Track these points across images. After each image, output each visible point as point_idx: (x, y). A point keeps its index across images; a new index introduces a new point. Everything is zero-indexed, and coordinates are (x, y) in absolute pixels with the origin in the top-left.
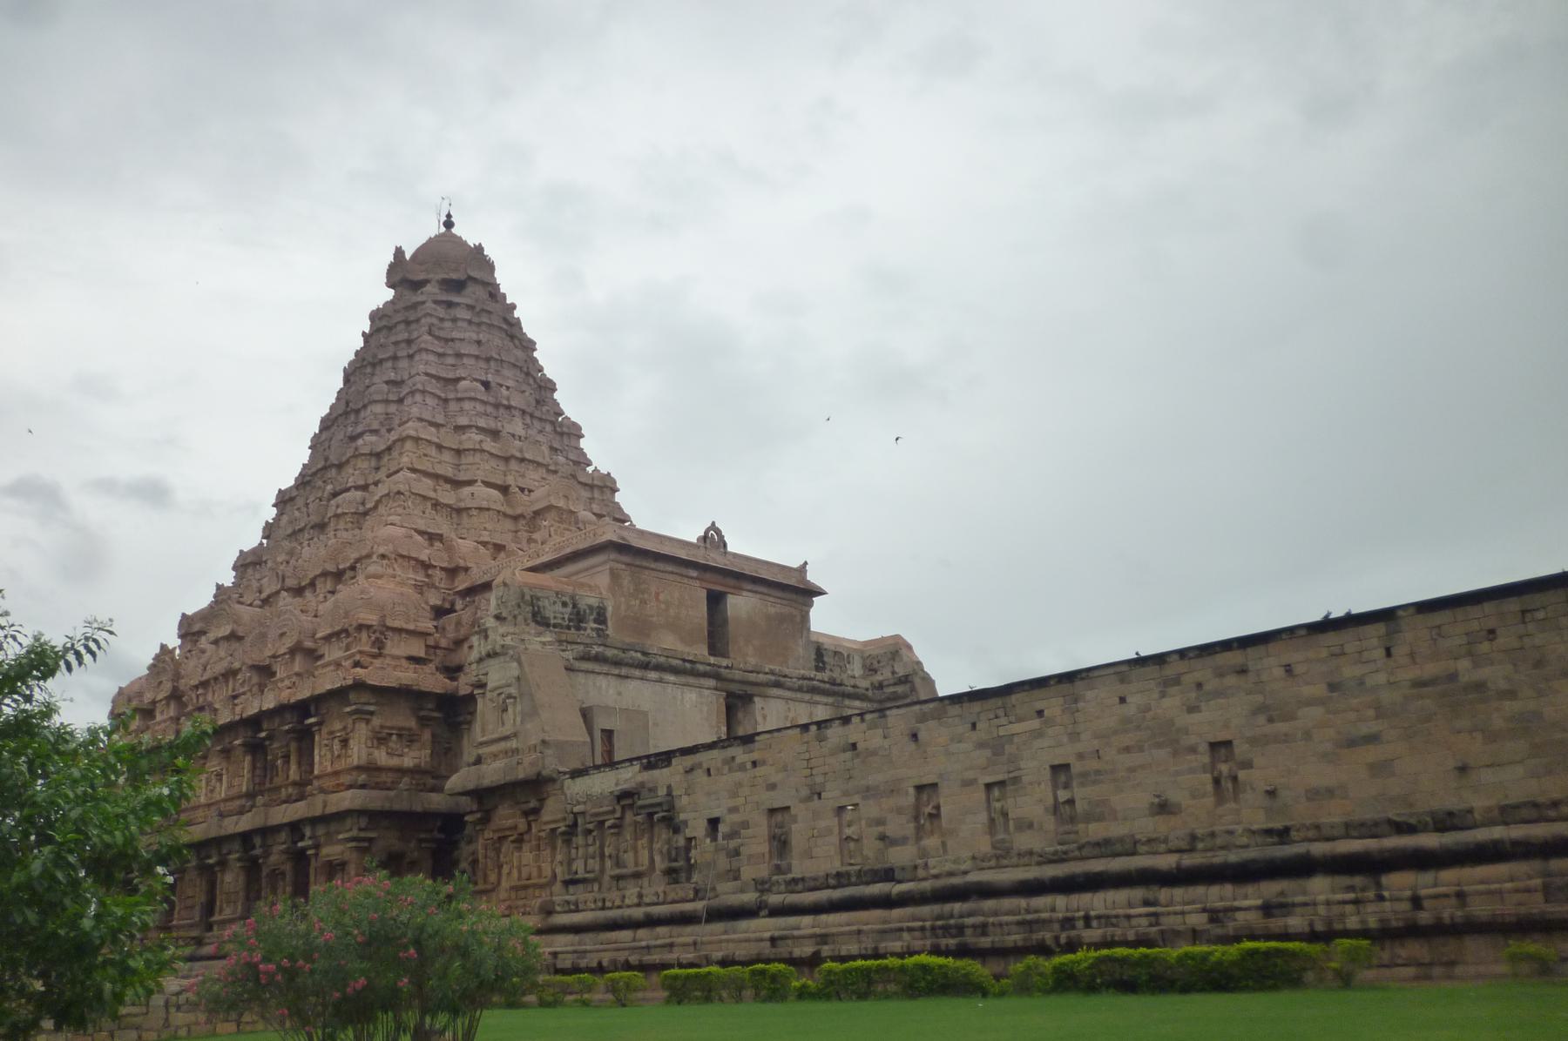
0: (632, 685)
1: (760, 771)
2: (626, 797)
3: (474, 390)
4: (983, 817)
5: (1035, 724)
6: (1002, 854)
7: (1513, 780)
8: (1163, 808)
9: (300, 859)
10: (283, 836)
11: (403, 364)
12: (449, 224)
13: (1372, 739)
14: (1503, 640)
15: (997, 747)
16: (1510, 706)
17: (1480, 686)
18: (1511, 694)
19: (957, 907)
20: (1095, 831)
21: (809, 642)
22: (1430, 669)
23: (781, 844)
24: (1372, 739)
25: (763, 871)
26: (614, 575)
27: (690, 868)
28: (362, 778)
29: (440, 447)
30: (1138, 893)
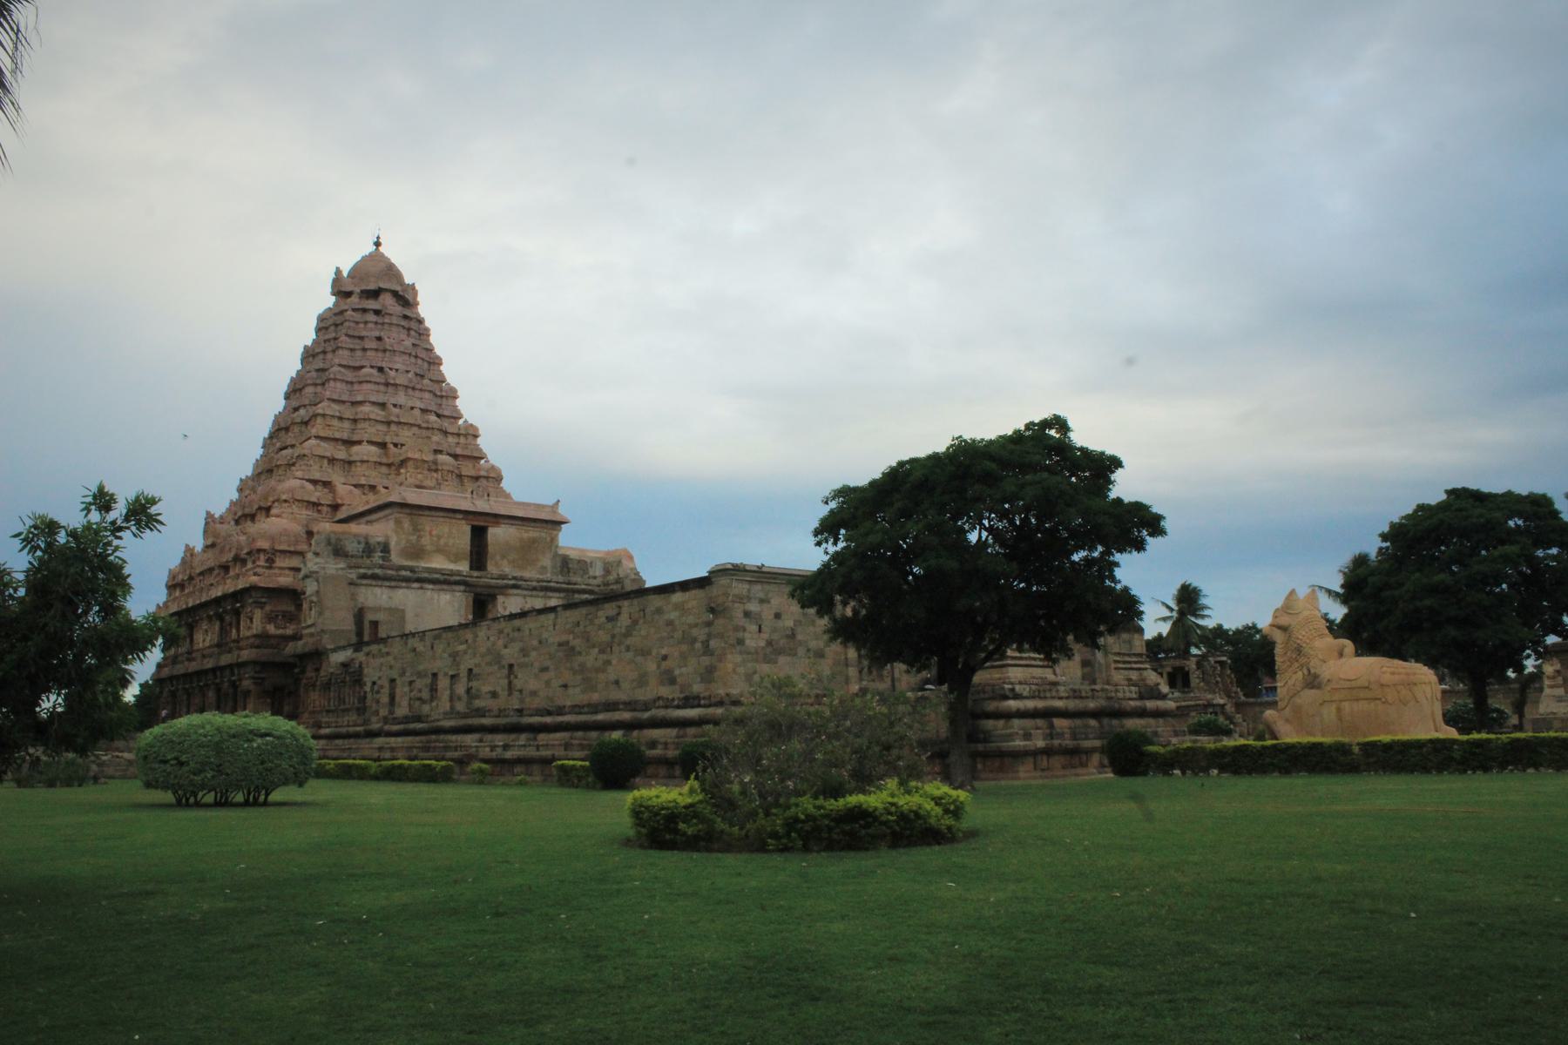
1: (390, 658)
2: (345, 665)
3: (371, 375)
5: (463, 647)
6: (452, 713)
7: (576, 696)
8: (494, 695)
9: (234, 685)
10: (227, 672)
11: (329, 356)
12: (378, 244)
15: (454, 655)
16: (580, 659)
17: (573, 648)
20: (478, 703)
21: (556, 554)
22: (564, 638)
23: (392, 697)
25: (383, 712)
26: (398, 522)
28: (257, 642)
29: (341, 418)
30: (476, 736)
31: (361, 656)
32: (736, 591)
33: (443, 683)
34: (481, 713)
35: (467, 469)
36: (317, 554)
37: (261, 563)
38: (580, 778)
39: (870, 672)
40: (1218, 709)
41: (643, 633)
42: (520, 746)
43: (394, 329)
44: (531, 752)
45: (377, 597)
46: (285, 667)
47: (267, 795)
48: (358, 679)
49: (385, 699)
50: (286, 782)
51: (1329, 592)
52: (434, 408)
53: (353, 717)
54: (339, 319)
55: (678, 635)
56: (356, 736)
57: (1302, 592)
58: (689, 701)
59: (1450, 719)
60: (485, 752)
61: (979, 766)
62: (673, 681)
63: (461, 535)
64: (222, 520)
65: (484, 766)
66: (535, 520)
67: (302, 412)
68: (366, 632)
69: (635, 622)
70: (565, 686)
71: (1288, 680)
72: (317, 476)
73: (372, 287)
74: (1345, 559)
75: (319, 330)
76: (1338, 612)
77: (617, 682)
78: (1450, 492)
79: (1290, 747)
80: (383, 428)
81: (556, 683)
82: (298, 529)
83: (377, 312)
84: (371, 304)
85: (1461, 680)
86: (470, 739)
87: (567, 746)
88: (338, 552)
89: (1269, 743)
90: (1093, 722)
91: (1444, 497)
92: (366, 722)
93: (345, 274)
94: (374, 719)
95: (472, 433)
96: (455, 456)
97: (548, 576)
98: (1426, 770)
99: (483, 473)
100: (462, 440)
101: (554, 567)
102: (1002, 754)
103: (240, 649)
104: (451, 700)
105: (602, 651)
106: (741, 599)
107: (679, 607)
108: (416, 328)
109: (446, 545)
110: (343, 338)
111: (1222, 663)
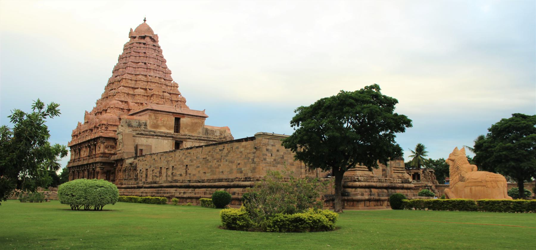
0: (150, 139)
2: (131, 164)
4: (165, 174)
6: (167, 181)
7: (208, 176)
9: (93, 170)
11: (128, 58)
12: (145, 20)
13: (199, 167)
14: (211, 153)
15: (168, 161)
16: (210, 164)
17: (208, 160)
18: (210, 162)
19: (160, 189)
20: (175, 178)
21: (204, 128)
22: (205, 156)
23: (147, 175)
24: (199, 167)
25: (144, 180)
26: (150, 116)
27: (137, 179)
28: (102, 155)
29: (131, 80)
30: (174, 189)
31: (136, 161)
32: (264, 142)
33: (164, 171)
34: (176, 181)
35: (174, 98)
36: (122, 126)
37: (104, 128)
38: (209, 204)
39: (309, 171)
40: (429, 188)
41: (232, 155)
42: (189, 193)
43: (150, 49)
44: (193, 195)
45: (142, 141)
46: (111, 164)
47: (102, 207)
48: (135, 169)
49: (144, 176)
50: (108, 203)
51: (470, 148)
52: (163, 77)
53: (133, 182)
54: (131, 46)
55: (243, 156)
56: (134, 188)
57: (460, 148)
58: (246, 179)
59: (510, 194)
60: (177, 195)
61: (346, 204)
62: (241, 172)
63: (171, 121)
64: (91, 114)
65: (177, 199)
66: (197, 116)
67: (118, 77)
68: (138, 153)
69: (229, 152)
70: (205, 173)
71: (453, 178)
72: (123, 99)
73: (143, 35)
74: (476, 137)
75: (124, 50)
76: (472, 155)
77: (222, 172)
78: (514, 115)
79: (454, 201)
80: (146, 83)
81: (202, 172)
82: (117, 118)
83: (144, 44)
84: (143, 41)
85: (515, 180)
86: (172, 190)
87: (205, 193)
88: (130, 126)
89: (446, 200)
90: (385, 191)
91: (511, 116)
92: (138, 183)
93: (134, 31)
94: (140, 182)
95: (176, 86)
96: (170, 94)
97: (201, 135)
98: (500, 211)
99: (179, 100)
100: (173, 88)
101: (203, 132)
102: (353, 201)
103: (95, 157)
104: (166, 176)
105: (218, 161)
106: (265, 145)
107: (244, 147)
108: (157, 49)
109: (166, 124)
110: (133, 52)
111: (431, 172)
